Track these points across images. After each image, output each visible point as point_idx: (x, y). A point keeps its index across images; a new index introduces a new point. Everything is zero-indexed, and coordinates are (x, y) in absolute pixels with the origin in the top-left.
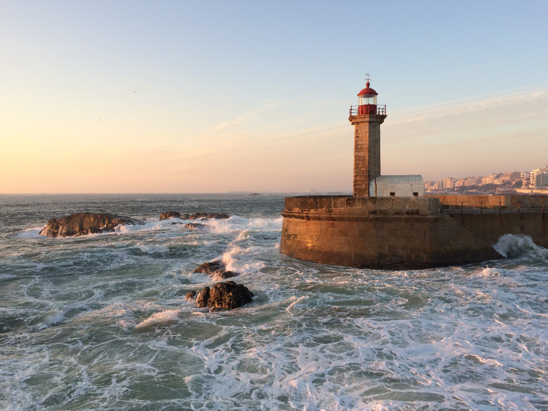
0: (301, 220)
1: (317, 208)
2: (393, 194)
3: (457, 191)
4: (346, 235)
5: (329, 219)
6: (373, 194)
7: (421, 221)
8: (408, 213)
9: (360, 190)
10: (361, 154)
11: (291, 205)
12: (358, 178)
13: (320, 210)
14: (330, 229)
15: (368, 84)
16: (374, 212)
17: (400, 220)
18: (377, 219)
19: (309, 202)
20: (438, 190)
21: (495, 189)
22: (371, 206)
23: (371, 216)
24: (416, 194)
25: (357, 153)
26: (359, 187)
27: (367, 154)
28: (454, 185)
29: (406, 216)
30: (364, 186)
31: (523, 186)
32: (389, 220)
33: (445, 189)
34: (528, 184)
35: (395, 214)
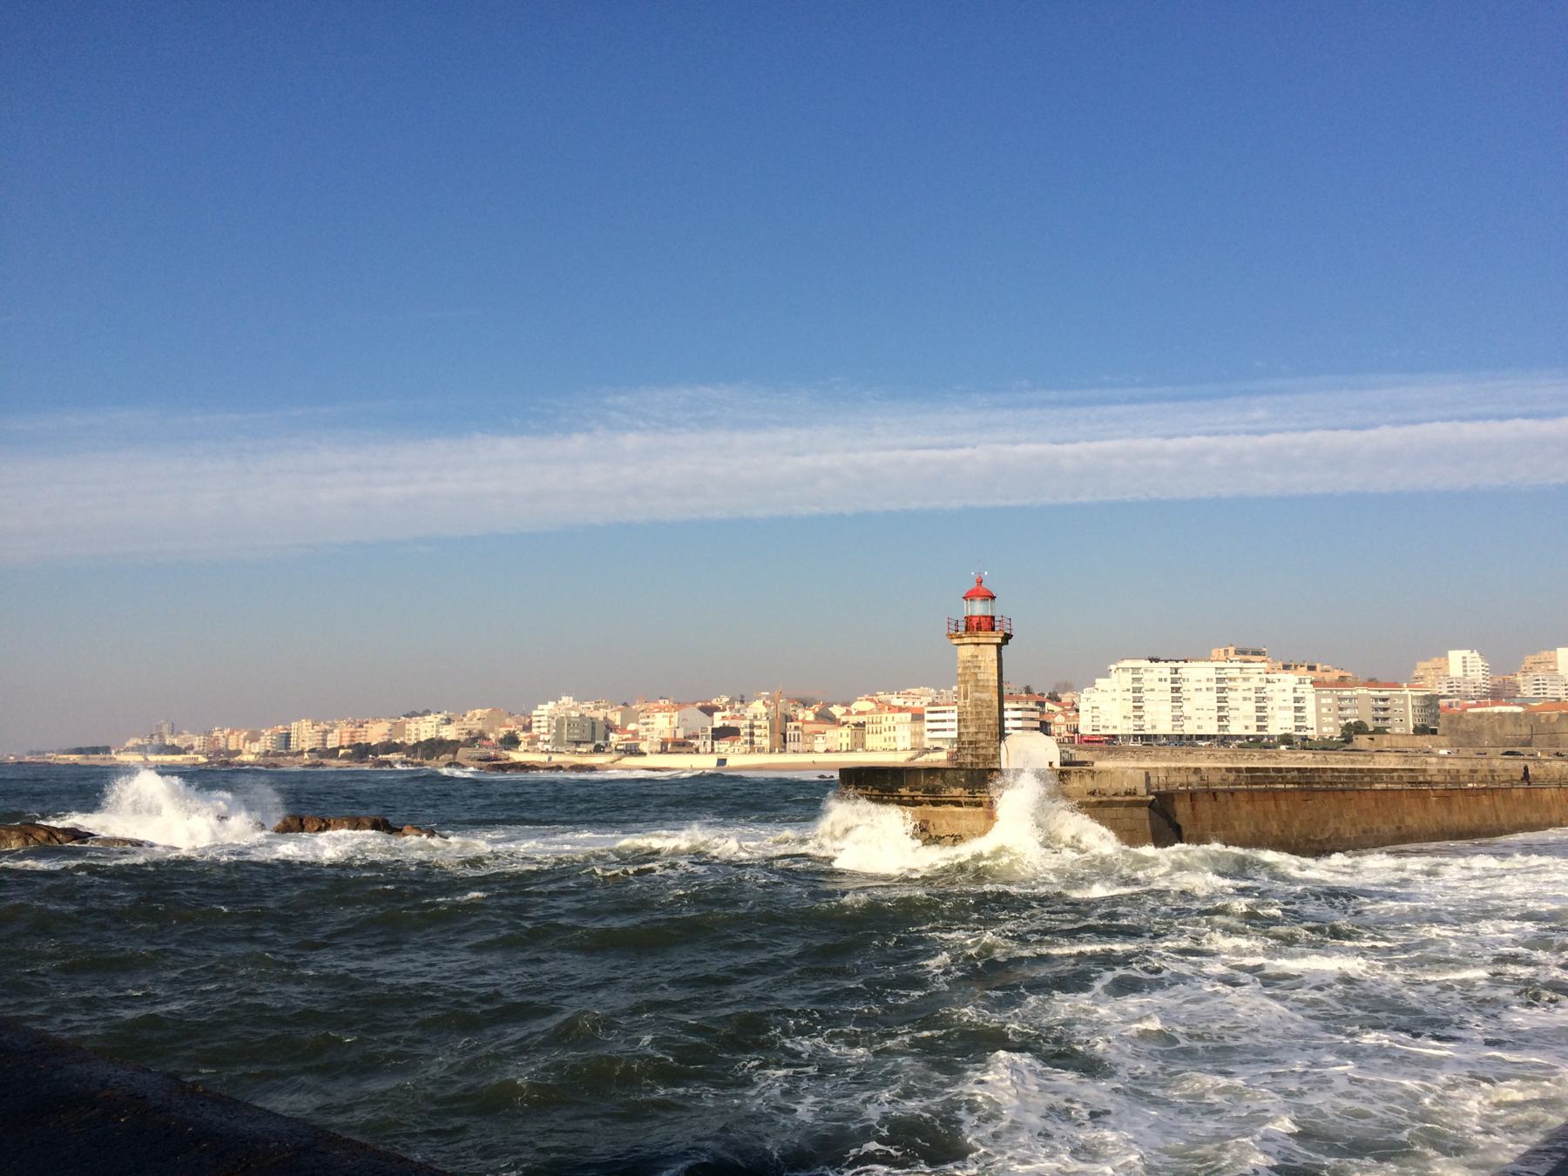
0: (971, 810)
3: (344, 757)
7: (1139, 804)
8: (1127, 794)
9: (986, 758)
10: (985, 696)
11: (938, 782)
12: (981, 737)
16: (1093, 793)
17: (1120, 804)
18: (1100, 803)
20: (276, 755)
21: (455, 753)
22: (1090, 784)
23: (1093, 799)
25: (978, 695)
26: (982, 752)
27: (996, 698)
28: (325, 740)
29: (1128, 798)
30: (991, 751)
31: (523, 747)
33: (301, 753)
34: (534, 740)
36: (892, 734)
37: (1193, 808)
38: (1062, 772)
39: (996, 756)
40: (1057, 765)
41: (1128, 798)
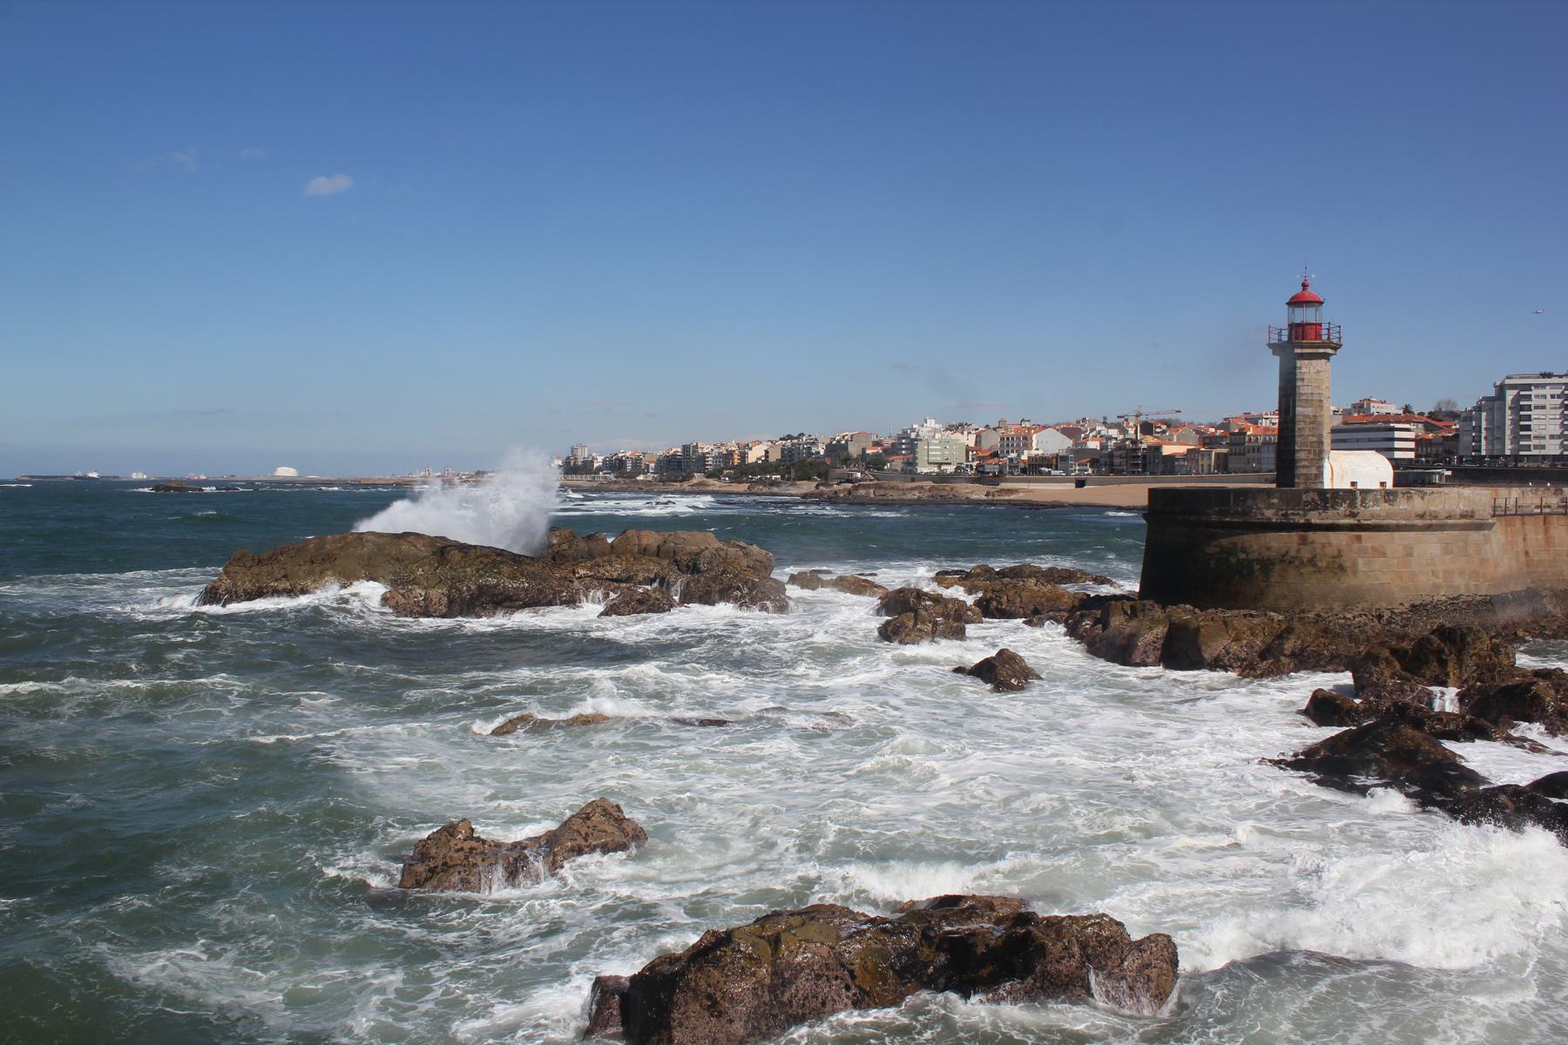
1: (1326, 508)
2: (1353, 484)
4: (1384, 555)
5: (1351, 528)
6: (1327, 485)
8: (1462, 516)
13: (1331, 512)
14: (1356, 546)
15: (1304, 286)
16: (1422, 516)
19: (1304, 497)
24: (1383, 484)
29: (1462, 521)
30: (1314, 471)
32: (1442, 528)
35: (1449, 517)
36: (1256, 455)
37: (1546, 531)
38: (1388, 493)
39: (1319, 475)
40: (1389, 486)
41: (1462, 521)
